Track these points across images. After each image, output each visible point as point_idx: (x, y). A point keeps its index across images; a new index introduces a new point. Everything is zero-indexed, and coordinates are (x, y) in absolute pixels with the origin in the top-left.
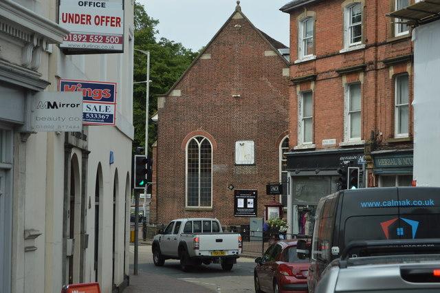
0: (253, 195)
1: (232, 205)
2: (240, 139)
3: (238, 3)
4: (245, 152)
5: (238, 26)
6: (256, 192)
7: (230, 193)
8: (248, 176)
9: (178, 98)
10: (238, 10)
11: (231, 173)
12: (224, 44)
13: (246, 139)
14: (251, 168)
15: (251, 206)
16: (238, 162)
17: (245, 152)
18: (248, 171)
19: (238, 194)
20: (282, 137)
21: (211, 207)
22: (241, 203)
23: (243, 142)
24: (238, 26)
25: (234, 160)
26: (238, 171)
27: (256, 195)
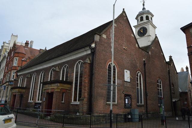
0: (130, 97)
1: (124, 102)
3: (124, 9)
5: (123, 17)
6: (131, 95)
7: (123, 95)
8: (128, 87)
10: (124, 12)
13: (127, 69)
14: (129, 83)
16: (125, 80)
18: (128, 85)
19: (126, 96)
20: (137, 72)
21: (116, 103)
22: (127, 102)
24: (123, 17)
27: (131, 97)
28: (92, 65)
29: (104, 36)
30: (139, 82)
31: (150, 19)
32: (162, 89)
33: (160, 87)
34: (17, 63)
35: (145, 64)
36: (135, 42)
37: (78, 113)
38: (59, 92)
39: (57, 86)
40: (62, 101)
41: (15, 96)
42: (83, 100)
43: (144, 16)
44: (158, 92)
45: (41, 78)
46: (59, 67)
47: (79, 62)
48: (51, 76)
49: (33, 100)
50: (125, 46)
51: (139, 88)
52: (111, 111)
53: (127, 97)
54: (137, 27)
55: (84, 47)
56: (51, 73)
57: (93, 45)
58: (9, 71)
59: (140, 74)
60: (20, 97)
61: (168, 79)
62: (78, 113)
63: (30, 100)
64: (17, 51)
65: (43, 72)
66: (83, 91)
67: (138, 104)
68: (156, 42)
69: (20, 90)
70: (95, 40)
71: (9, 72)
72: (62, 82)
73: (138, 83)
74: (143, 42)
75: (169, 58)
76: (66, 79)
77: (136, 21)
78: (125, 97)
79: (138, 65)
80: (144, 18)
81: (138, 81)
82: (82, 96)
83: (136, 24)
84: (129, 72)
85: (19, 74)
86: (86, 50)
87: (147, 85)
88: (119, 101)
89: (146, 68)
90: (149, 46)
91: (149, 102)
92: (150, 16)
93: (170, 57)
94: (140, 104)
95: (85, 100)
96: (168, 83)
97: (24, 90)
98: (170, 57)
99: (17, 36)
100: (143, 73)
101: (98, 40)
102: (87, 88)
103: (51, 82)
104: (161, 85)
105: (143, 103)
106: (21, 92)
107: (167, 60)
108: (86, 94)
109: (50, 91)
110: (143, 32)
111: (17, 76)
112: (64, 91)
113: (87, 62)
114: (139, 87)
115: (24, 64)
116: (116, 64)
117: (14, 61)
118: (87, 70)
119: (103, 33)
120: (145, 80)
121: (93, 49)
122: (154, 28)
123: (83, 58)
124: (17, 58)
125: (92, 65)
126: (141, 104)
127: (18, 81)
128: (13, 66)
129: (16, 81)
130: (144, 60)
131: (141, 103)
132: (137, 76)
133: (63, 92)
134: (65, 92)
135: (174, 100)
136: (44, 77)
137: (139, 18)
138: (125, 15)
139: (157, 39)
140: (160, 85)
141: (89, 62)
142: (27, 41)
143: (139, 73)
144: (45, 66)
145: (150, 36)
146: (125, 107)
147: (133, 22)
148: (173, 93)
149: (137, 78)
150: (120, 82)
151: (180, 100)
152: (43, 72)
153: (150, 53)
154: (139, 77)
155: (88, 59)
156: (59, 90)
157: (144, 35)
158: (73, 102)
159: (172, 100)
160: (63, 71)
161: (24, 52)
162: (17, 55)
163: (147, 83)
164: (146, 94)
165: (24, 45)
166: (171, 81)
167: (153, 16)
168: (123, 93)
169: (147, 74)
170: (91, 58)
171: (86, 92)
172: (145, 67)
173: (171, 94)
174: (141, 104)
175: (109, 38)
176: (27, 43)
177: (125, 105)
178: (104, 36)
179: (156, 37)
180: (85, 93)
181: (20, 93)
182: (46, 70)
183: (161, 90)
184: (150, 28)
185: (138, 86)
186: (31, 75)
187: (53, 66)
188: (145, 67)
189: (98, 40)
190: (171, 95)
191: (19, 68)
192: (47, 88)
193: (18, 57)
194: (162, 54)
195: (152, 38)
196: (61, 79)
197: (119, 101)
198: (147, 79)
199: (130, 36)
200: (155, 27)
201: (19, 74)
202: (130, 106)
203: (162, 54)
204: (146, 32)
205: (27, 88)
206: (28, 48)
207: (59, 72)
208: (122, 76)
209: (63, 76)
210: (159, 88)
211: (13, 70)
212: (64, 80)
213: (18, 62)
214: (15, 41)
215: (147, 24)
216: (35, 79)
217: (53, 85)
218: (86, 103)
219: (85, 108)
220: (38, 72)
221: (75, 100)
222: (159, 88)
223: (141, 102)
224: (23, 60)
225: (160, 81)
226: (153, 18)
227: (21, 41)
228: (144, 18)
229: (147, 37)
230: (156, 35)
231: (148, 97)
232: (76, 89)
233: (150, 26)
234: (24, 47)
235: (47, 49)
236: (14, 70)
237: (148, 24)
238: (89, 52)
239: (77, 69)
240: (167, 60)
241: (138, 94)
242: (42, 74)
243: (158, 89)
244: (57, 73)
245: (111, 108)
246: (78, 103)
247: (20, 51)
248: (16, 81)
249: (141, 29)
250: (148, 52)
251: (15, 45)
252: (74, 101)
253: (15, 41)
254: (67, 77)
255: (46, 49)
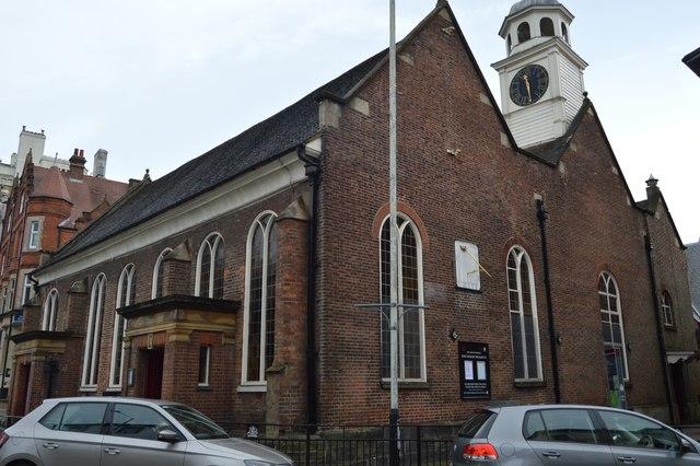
0: (483, 354)
1: (455, 374)
2: (460, 238)
4: (468, 266)
5: (441, 28)
6: (486, 345)
7: (451, 348)
8: (474, 313)
9: (364, 118)
11: (451, 302)
12: (431, 52)
13: (468, 240)
15: (482, 375)
16: (460, 285)
17: (468, 266)
18: (473, 303)
19: (470, 349)
20: (507, 247)
21: (424, 378)
22: (469, 375)
23: (464, 244)
25: (454, 277)
26: (461, 298)
27: (486, 354)
28: (310, 225)
29: (362, 107)
30: (519, 289)
31: (558, 31)
32: (619, 313)
33: (614, 308)
34: (38, 238)
35: (541, 216)
36: (497, 124)
37: (253, 429)
38: (188, 345)
39: (177, 320)
40: (201, 380)
41: (26, 368)
42: (277, 372)
43: (534, 23)
44: (606, 327)
45: (124, 291)
46: (187, 243)
47: (262, 219)
48: (160, 280)
49: (95, 382)
50: (454, 146)
51: (522, 315)
52: (394, 415)
53: (471, 354)
54: (506, 67)
55: (277, 156)
56: (161, 271)
57: (315, 146)
58: (11, 272)
59: (523, 258)
60: (45, 372)
61: (645, 270)
62: (253, 429)
63: (88, 382)
64: (37, 192)
65: (129, 269)
66: (279, 336)
67: (517, 380)
68: (587, 123)
69: (46, 344)
70: (322, 123)
71: (13, 276)
72: (202, 304)
73: (514, 296)
74: (534, 127)
75: (646, 186)
76: (218, 292)
77: (504, 42)
78: (461, 353)
79: (512, 219)
80: (535, 30)
81: (513, 285)
82: (278, 358)
83: (503, 55)
84: (473, 250)
85: (42, 281)
86: (287, 169)
87: (555, 300)
88: (436, 371)
89: (547, 231)
90: (560, 139)
91: (565, 370)
92: (557, 21)
93: (652, 183)
94: (526, 378)
95: (291, 371)
96: (648, 288)
97: (61, 345)
98: (652, 183)
99: (41, 136)
100: (538, 250)
101: (335, 124)
102: (294, 324)
103: (151, 309)
104: (615, 299)
105: (541, 377)
106: (47, 354)
107: (639, 194)
108: (292, 348)
109: (149, 343)
110: (530, 85)
111: (37, 288)
112: (206, 339)
113: (291, 215)
114: (521, 311)
115: (67, 237)
116: (420, 220)
117: (27, 231)
118: (295, 250)
119: (355, 95)
120: (547, 282)
121: (314, 159)
122: (579, 67)
123: (273, 201)
124: (40, 219)
125: (310, 225)
126: (532, 379)
127: (40, 308)
128: (25, 250)
129: (33, 308)
130: (537, 196)
131: (530, 377)
132: (512, 264)
133: (200, 347)
134: (210, 345)
135: (672, 359)
136: (134, 288)
137: (514, 31)
138: (447, 17)
139: (590, 111)
140: (613, 301)
141: (299, 215)
142: (76, 150)
143: (518, 252)
144: (138, 243)
145: (560, 98)
146: (462, 395)
147: (488, 48)
148: (667, 329)
149: (512, 274)
150: (439, 290)
151: (698, 357)
152: (129, 269)
153: (562, 168)
154: (518, 270)
155: (295, 204)
156: (186, 338)
157: (535, 98)
158: (245, 385)
159: (663, 356)
160: (206, 258)
161: (66, 195)
162: (37, 207)
163: (553, 295)
164: (552, 340)
165: (67, 168)
166: (658, 282)
167: (569, 18)
168: (451, 336)
169: (553, 256)
170: (308, 198)
171: (291, 338)
172: (542, 226)
173: (659, 332)
174: (532, 379)
175: (380, 114)
176: (78, 160)
177: (463, 388)
178: (362, 107)
179: (587, 104)
180: (286, 344)
181: (43, 358)
182: (142, 259)
183: (615, 318)
184: (557, 66)
185: (515, 306)
186: (86, 281)
187: (166, 242)
188: (542, 226)
189: (335, 124)
190: (660, 339)
191: (41, 260)
192: (142, 331)
193: (41, 213)
194: (614, 170)
195: (573, 107)
196: (197, 293)
197: (436, 371)
198: (554, 276)
199: (475, 104)
200: (580, 64)
201: (42, 281)
202: (485, 390)
203: (614, 170)
204: (545, 85)
205: (74, 336)
206: (82, 177)
207: (190, 264)
208: (443, 267)
209: (205, 277)
210: (610, 312)
211: (23, 266)
212: (211, 296)
213: (43, 233)
214: (30, 154)
215: (545, 54)
216: (104, 296)
217: (160, 318)
218: (295, 384)
219: (294, 403)
220: (112, 268)
221: (253, 375)
222: (610, 312)
223: (533, 373)
224: (62, 224)
225: (611, 283)
226: (571, 28)
227: (57, 150)
228: (535, 30)
229: (546, 106)
230: (585, 94)
231: (561, 350)
232: (255, 328)
233: (561, 60)
234: (66, 174)
235: (154, 177)
236: (29, 266)
237: (550, 51)
238: (300, 174)
239: (262, 246)
240: (639, 194)
241: (517, 339)
242: (126, 276)
243: (605, 316)
244: (183, 268)
245: (394, 402)
246: (261, 385)
247: (48, 193)
248: (33, 308)
249: (522, 72)
250: (554, 167)
251: (29, 166)
252: (249, 379)
253: (30, 154)
254: (219, 283)
255: (147, 176)
